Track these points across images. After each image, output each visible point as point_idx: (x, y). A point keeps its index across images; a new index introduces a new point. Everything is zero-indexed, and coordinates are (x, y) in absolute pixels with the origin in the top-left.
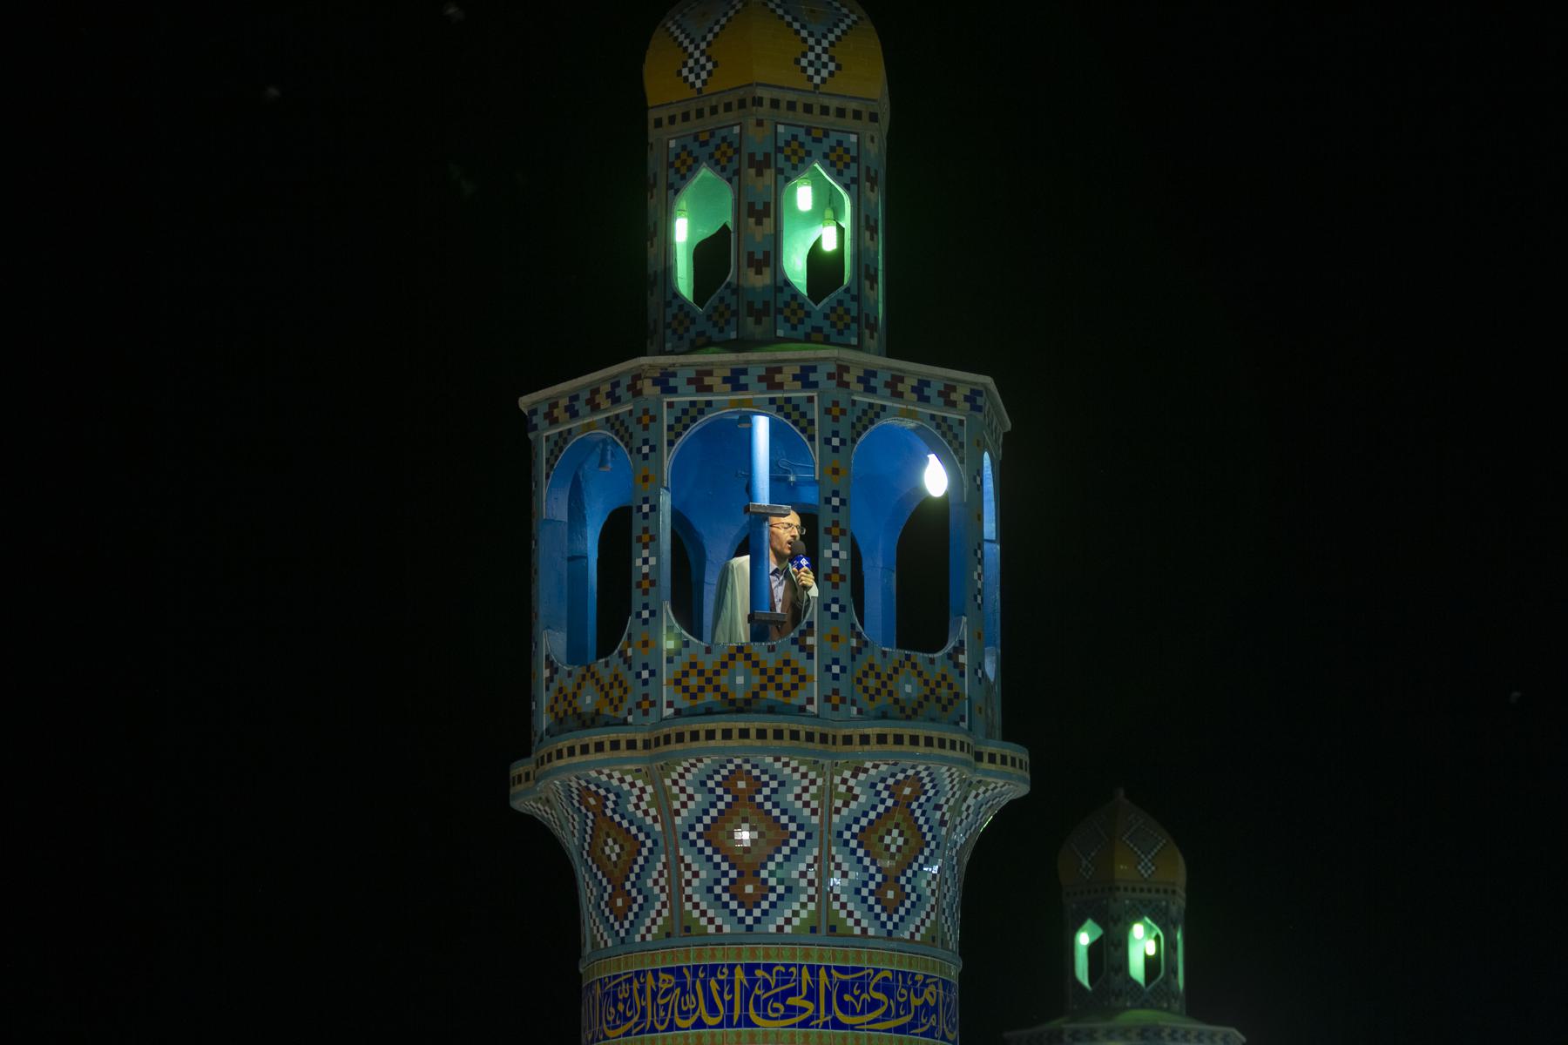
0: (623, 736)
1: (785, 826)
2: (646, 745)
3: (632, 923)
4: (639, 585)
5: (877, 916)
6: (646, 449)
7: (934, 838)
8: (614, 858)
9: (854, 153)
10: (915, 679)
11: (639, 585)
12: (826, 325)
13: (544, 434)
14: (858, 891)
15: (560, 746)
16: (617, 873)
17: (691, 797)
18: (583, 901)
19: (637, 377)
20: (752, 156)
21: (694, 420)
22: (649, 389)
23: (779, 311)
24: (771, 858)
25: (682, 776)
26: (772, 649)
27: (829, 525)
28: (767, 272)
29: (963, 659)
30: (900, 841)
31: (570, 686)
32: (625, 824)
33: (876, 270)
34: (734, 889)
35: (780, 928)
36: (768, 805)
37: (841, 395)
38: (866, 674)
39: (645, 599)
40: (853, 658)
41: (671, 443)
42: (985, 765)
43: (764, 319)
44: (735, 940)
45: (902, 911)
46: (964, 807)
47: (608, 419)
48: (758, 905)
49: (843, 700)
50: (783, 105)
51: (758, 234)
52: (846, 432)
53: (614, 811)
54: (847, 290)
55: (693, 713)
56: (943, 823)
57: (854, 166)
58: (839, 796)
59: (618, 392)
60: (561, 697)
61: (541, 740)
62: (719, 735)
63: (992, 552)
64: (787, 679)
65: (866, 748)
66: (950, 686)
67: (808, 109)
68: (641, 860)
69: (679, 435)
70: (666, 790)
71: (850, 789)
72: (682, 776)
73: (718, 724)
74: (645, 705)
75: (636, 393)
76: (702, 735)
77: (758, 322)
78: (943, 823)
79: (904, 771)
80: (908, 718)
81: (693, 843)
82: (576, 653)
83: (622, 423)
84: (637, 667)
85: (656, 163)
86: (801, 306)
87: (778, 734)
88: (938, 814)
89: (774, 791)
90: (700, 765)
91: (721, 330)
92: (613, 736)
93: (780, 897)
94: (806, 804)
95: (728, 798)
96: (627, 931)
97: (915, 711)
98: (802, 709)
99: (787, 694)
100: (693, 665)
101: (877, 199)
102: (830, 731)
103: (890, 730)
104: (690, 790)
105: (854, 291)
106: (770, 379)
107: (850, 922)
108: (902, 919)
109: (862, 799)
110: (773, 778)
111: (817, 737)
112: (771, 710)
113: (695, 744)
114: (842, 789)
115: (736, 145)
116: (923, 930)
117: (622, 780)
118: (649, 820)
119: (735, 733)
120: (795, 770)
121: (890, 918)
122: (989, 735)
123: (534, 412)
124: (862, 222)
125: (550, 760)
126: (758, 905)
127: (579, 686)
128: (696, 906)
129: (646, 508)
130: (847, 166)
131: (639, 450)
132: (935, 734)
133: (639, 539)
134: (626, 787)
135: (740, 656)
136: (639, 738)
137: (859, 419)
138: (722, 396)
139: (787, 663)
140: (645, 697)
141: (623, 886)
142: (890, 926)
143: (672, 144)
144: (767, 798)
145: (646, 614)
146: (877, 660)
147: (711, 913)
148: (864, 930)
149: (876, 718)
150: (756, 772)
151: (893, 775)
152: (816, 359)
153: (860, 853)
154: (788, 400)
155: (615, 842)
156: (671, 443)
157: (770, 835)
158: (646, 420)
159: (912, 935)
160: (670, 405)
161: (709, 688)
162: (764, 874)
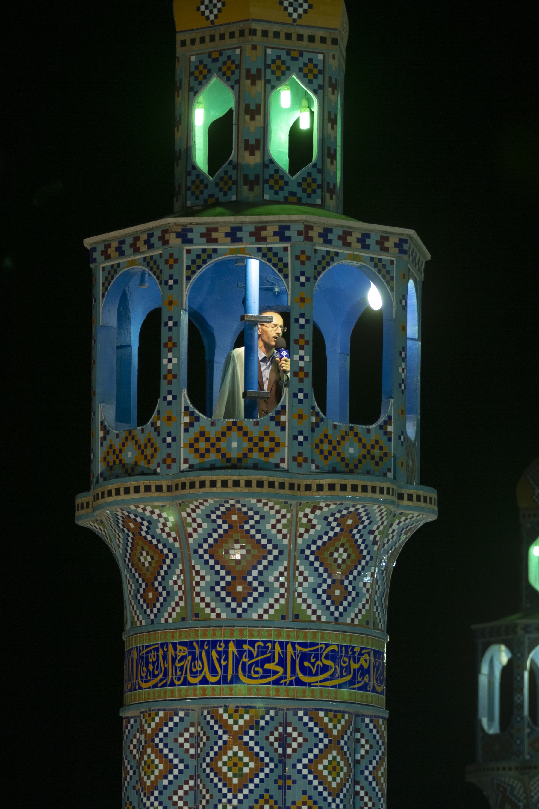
0: (153, 482)
1: (265, 546)
2: (169, 488)
3: (159, 610)
4: (165, 377)
5: (328, 608)
6: (171, 282)
7: (368, 553)
8: (147, 564)
9: (320, 67)
10: (357, 444)
11: (165, 377)
12: (299, 191)
13: (100, 266)
14: (315, 591)
15: (110, 487)
16: (149, 575)
17: (200, 525)
18: (126, 592)
19: (165, 232)
20: (248, 71)
21: (204, 262)
22: (174, 240)
23: (266, 181)
24: (255, 568)
25: (193, 511)
26: (256, 424)
28: (258, 154)
29: (390, 429)
30: (345, 556)
31: (117, 444)
32: (155, 542)
33: (335, 150)
34: (229, 589)
35: (260, 616)
36: (253, 532)
37: (307, 247)
38: (321, 441)
39: (170, 387)
40: (313, 430)
41: (188, 278)
42: (405, 502)
43: (256, 187)
44: (229, 624)
45: (345, 604)
46: (390, 531)
47: (145, 259)
48: (245, 600)
49: (305, 460)
51: (251, 127)
52: (310, 272)
53: (147, 533)
54: (314, 166)
55: (202, 468)
56: (375, 542)
57: (320, 76)
58: (302, 525)
59: (152, 240)
60: (111, 451)
61: (97, 482)
62: (219, 484)
63: (414, 348)
64: (267, 444)
65: (321, 493)
66: (381, 448)
68: (165, 567)
69: (194, 272)
71: (310, 521)
72: (193, 511)
73: (219, 476)
74: (169, 461)
75: (166, 243)
76: (208, 484)
77: (251, 189)
78: (375, 542)
79: (347, 508)
80: (351, 472)
81: (201, 557)
82: (122, 416)
83: (155, 262)
84: (164, 434)
85: (181, 72)
86: (282, 177)
87: (260, 484)
88: (372, 537)
89: (257, 522)
90: (206, 504)
91: (225, 194)
92: (147, 482)
93: (261, 595)
94: (279, 531)
95: (225, 526)
96: (155, 615)
97: (356, 466)
98: (277, 466)
99: (266, 455)
100: (202, 434)
101: (338, 100)
102: (296, 482)
103: (338, 480)
104: (199, 520)
105: (319, 167)
106: (257, 234)
107: (309, 612)
108: (345, 609)
109: (318, 527)
110: (256, 513)
111: (287, 486)
112: (256, 467)
113: (202, 490)
114: (304, 520)
115: (237, 62)
116: (360, 616)
117: (152, 512)
118: (171, 540)
119: (230, 483)
120: (272, 508)
121: (337, 609)
122: (409, 482)
123: (94, 249)
124: (327, 118)
125: (103, 497)
126: (245, 600)
127: (124, 445)
128: (203, 600)
129: (171, 324)
130: (315, 77)
131: (166, 283)
132: (369, 484)
133: (166, 345)
134: (155, 517)
135: (235, 428)
137: (320, 262)
138: (225, 247)
139: (267, 433)
140: (169, 455)
141: (153, 584)
142: (337, 614)
143: (193, 59)
144: (252, 527)
145: (170, 398)
146: (330, 432)
147: (213, 605)
148: (319, 618)
149: (329, 472)
150: (244, 509)
151: (340, 511)
152: (290, 221)
153: (317, 564)
154: (270, 249)
155: (148, 554)
157: (255, 552)
158: (171, 261)
159: (352, 620)
160: (188, 251)
161: (213, 450)
162: (250, 578)
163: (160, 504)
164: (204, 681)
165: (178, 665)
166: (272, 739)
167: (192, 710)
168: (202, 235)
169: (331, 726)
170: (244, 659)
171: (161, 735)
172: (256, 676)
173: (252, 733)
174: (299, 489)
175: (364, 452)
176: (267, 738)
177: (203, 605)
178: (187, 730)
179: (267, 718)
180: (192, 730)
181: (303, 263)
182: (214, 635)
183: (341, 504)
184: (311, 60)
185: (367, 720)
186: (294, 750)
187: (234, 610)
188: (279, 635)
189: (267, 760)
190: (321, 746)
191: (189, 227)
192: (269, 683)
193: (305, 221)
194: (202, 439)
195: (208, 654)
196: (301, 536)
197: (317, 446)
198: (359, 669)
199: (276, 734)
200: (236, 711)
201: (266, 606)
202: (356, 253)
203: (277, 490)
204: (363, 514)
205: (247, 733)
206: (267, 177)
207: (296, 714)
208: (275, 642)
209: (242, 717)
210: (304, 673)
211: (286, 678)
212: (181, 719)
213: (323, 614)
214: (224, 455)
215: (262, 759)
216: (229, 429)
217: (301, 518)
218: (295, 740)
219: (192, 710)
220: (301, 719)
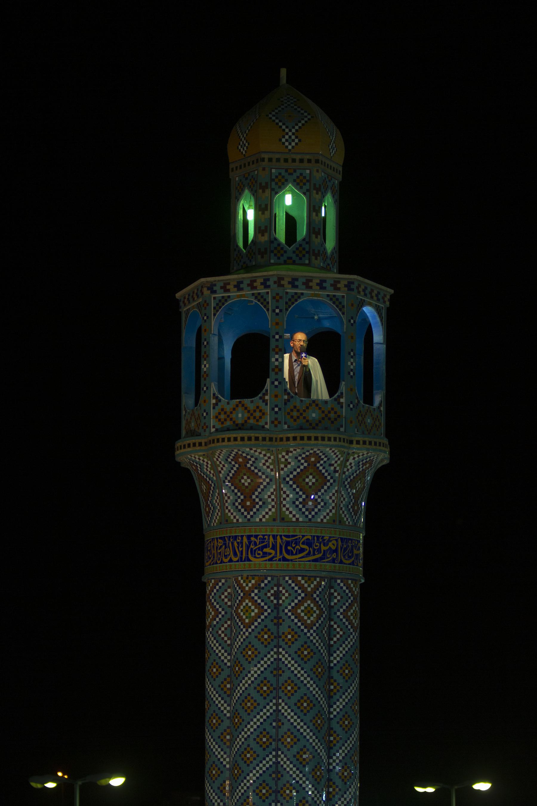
2: (206, 444)
9: (308, 178)
14: (294, 503)
20: (261, 184)
22: (206, 292)
26: (252, 402)
27: (274, 347)
30: (314, 480)
34: (243, 504)
35: (261, 520)
38: (292, 410)
40: (285, 404)
41: (215, 315)
50: (274, 160)
56: (335, 471)
57: (308, 184)
58: (282, 463)
64: (258, 414)
66: (336, 413)
67: (286, 160)
70: (215, 462)
71: (286, 460)
72: (219, 457)
73: (232, 435)
77: (262, 257)
78: (335, 471)
80: (314, 428)
86: (282, 248)
87: (250, 439)
88: (332, 468)
93: (261, 506)
94: (268, 467)
97: (317, 425)
98: (263, 427)
100: (222, 410)
102: (274, 436)
107: (291, 516)
109: (293, 464)
110: (252, 457)
112: (252, 428)
114: (283, 460)
116: (328, 517)
119: (232, 439)
120: (260, 453)
134: (202, 462)
136: (203, 441)
137: (290, 300)
139: (258, 407)
143: (237, 179)
146: (298, 404)
149: (297, 429)
150: (244, 455)
153: (294, 486)
154: (259, 294)
156: (215, 315)
160: (214, 298)
163: (202, 454)
164: (231, 561)
165: (219, 551)
166: (269, 594)
167: (229, 578)
168: (221, 288)
169: (306, 585)
170: (252, 546)
171: (213, 594)
172: (258, 556)
173: (256, 591)
174: (276, 440)
175: (323, 415)
176: (266, 594)
177: (287, 512)
178: (226, 591)
179: (266, 582)
180: (229, 590)
181: (277, 301)
182: (235, 532)
183: (303, 449)
184: (301, 174)
185: (339, 581)
186: (283, 601)
187: (307, 516)
188: (272, 531)
189: (266, 607)
190: (299, 598)
191: (214, 283)
192: (266, 561)
193: (278, 275)
194: (222, 413)
195: (232, 544)
196: (282, 469)
197: (289, 414)
198: (327, 550)
199: (272, 592)
200: (247, 578)
201: (264, 513)
202: (316, 292)
203: (261, 442)
204: (233, 455)
205: (253, 592)
206: (272, 249)
207: (284, 579)
208: (269, 535)
209: (250, 582)
210: (289, 554)
211: (276, 557)
212: (223, 584)
213: (300, 517)
214: (234, 422)
215: (263, 607)
216: (237, 406)
217: (280, 459)
218: (284, 595)
219: (229, 578)
220: (287, 582)
